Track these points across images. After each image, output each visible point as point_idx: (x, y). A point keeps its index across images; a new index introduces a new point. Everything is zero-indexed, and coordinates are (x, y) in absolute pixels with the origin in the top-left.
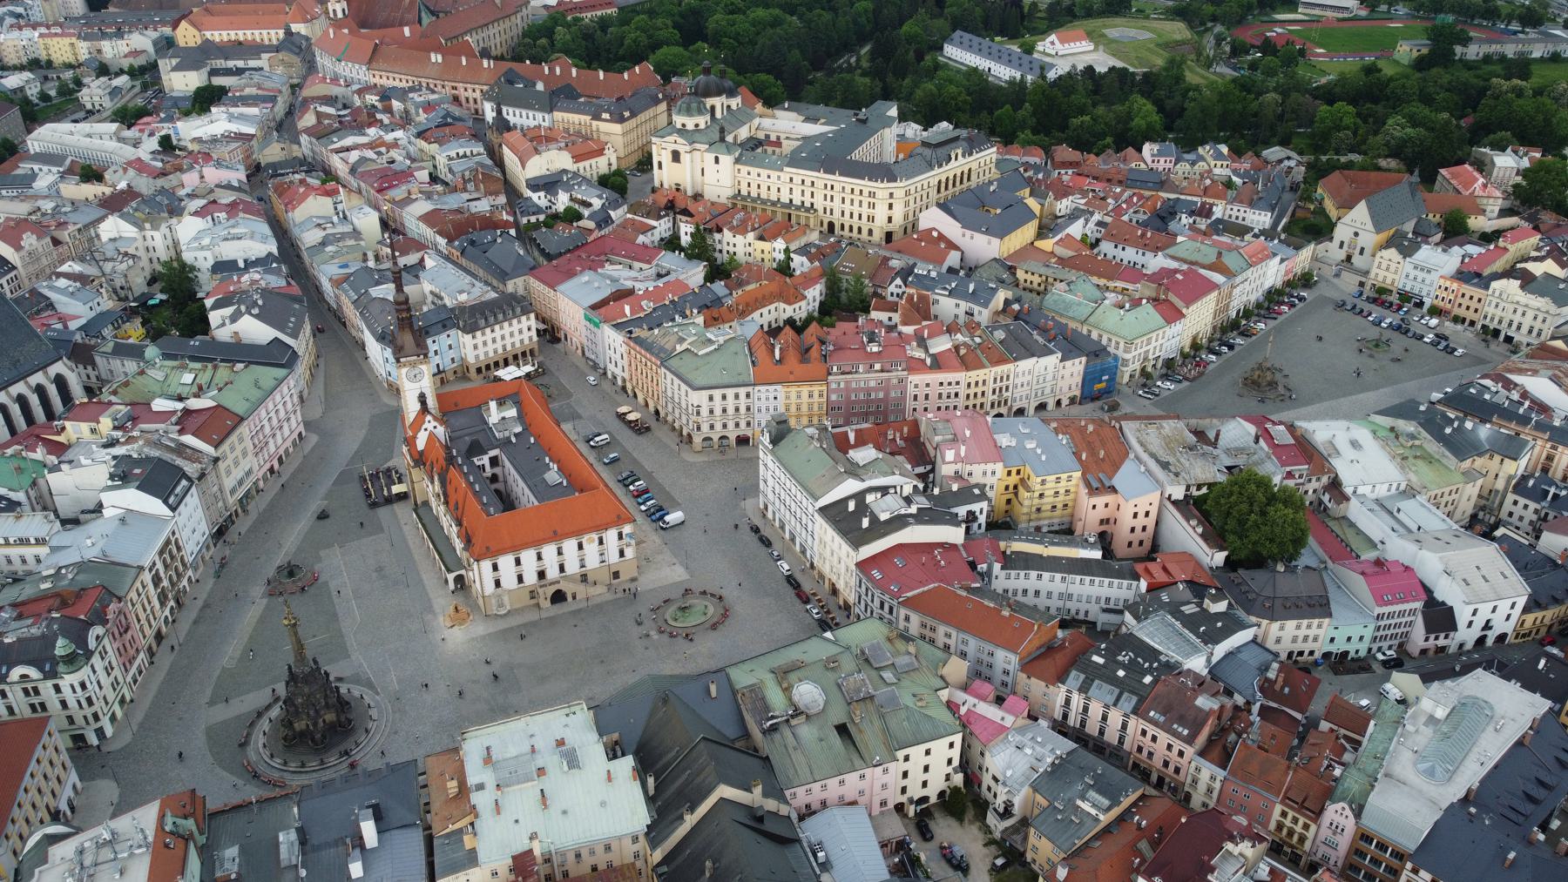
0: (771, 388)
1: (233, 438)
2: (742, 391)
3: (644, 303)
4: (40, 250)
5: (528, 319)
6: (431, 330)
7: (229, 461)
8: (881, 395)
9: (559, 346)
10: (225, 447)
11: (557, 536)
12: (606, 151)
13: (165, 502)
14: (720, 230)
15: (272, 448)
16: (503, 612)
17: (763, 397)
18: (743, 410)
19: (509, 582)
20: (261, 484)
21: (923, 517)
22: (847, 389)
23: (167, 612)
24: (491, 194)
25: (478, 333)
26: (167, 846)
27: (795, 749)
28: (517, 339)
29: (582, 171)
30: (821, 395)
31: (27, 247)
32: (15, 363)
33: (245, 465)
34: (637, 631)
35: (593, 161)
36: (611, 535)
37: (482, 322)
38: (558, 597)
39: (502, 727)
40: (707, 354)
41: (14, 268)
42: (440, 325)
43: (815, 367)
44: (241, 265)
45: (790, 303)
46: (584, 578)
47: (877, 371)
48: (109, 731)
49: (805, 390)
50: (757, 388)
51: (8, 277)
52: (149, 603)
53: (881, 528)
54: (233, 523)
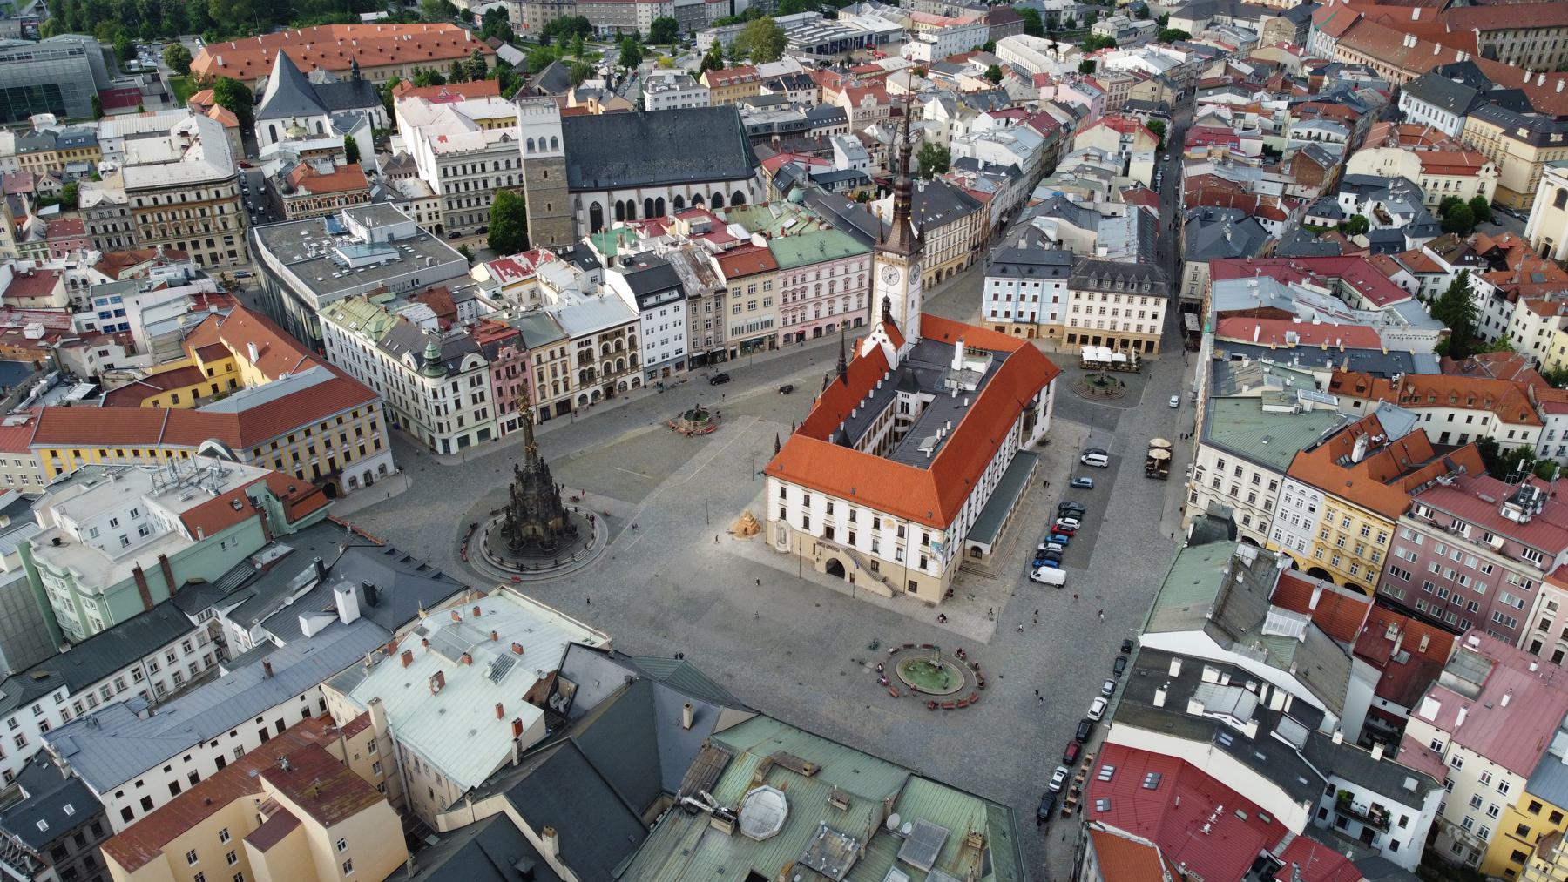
0: (1310, 492)
1: (759, 281)
2: (1267, 476)
3: (1290, 334)
4: (876, 113)
5: (1157, 303)
6: (1037, 271)
7: (745, 299)
8: (1481, 589)
9: (1191, 355)
10: (744, 285)
11: (853, 496)
12: (1482, 173)
13: (640, 299)
14: (1514, 301)
15: (810, 315)
16: (781, 548)
17: (1295, 497)
18: (1260, 503)
19: (795, 519)
20: (780, 342)
21: (1240, 748)
22: (1427, 553)
23: (589, 392)
24: (1303, 184)
25: (1084, 295)
26: (232, 504)
27: (686, 852)
28: (1134, 321)
29: (1430, 186)
30: (1381, 539)
31: (864, 107)
32: (708, 167)
33: (762, 314)
34: (861, 651)
35: (1453, 180)
36: (915, 531)
37: (1093, 284)
38: (836, 569)
39: (532, 607)
40: (1276, 414)
41: (847, 121)
42: (1051, 270)
43: (1395, 494)
44: (981, 166)
45: (1505, 420)
46: (875, 566)
47: (1492, 549)
48: (454, 447)
49: (1359, 519)
50: (1288, 481)
51: (837, 127)
52: (565, 372)
53: (1174, 720)
54: (725, 360)
